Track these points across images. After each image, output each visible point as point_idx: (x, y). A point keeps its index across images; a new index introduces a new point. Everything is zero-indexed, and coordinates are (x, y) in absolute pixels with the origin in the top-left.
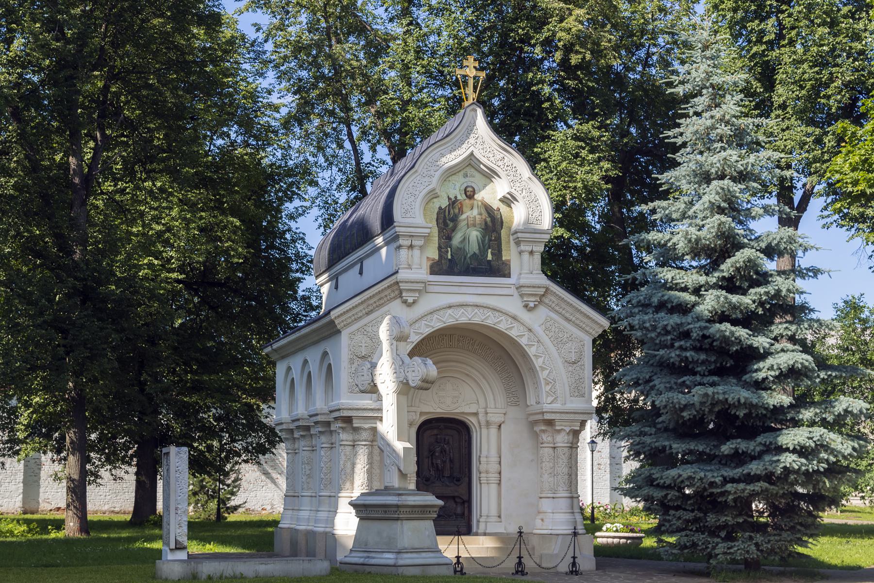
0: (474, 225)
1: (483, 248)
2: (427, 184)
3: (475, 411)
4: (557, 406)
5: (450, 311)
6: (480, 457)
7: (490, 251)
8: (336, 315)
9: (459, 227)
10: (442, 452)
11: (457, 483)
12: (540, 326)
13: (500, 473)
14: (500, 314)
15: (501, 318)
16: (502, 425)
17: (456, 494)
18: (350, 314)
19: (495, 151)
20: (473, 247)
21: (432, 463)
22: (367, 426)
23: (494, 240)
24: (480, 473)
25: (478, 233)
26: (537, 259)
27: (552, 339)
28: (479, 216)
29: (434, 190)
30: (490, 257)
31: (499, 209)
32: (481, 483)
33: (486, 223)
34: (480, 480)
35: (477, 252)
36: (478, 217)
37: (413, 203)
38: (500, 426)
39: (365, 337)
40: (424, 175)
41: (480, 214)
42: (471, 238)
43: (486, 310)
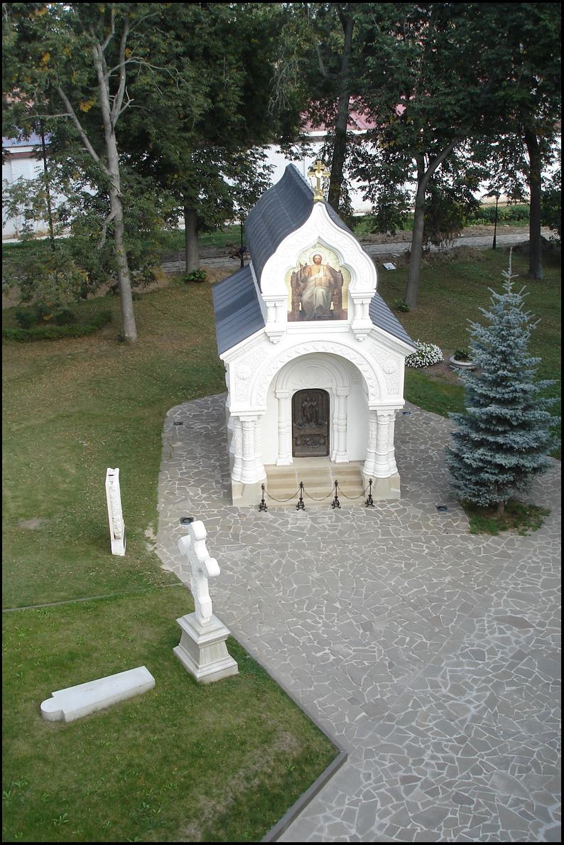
1: (327, 300)
4: (377, 402)
5: (303, 345)
7: (332, 303)
9: (309, 285)
20: (320, 301)
22: (248, 420)
25: (323, 290)
26: (367, 308)
30: (332, 308)
31: (340, 271)
33: (330, 283)
35: (322, 304)
36: (324, 278)
41: (326, 276)
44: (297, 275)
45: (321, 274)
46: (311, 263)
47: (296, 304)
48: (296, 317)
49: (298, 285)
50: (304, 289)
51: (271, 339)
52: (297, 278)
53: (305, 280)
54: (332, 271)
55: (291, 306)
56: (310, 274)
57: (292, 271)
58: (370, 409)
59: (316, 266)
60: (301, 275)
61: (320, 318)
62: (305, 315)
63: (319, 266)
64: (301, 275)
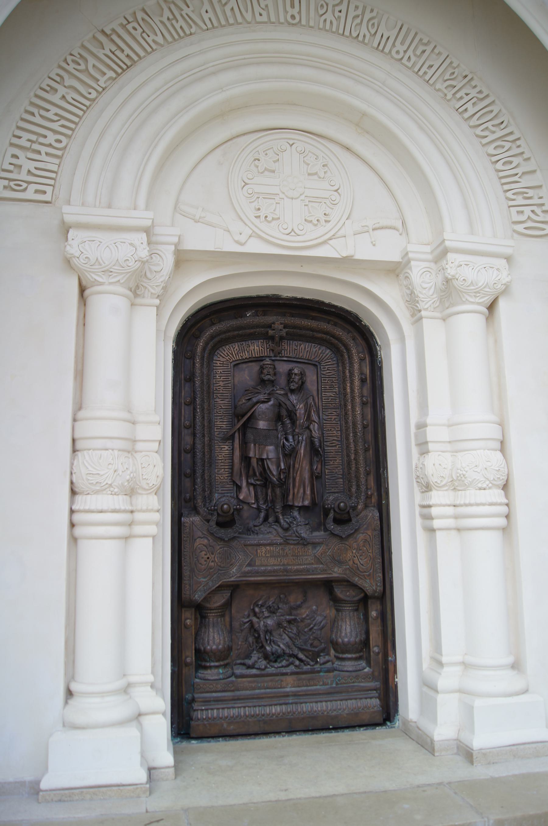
3: (396, 257)
6: (421, 426)
10: (279, 418)
11: (337, 530)
16: (502, 304)
17: (337, 572)
21: (246, 459)
24: (427, 488)
32: (431, 531)
34: (428, 517)
38: (492, 307)
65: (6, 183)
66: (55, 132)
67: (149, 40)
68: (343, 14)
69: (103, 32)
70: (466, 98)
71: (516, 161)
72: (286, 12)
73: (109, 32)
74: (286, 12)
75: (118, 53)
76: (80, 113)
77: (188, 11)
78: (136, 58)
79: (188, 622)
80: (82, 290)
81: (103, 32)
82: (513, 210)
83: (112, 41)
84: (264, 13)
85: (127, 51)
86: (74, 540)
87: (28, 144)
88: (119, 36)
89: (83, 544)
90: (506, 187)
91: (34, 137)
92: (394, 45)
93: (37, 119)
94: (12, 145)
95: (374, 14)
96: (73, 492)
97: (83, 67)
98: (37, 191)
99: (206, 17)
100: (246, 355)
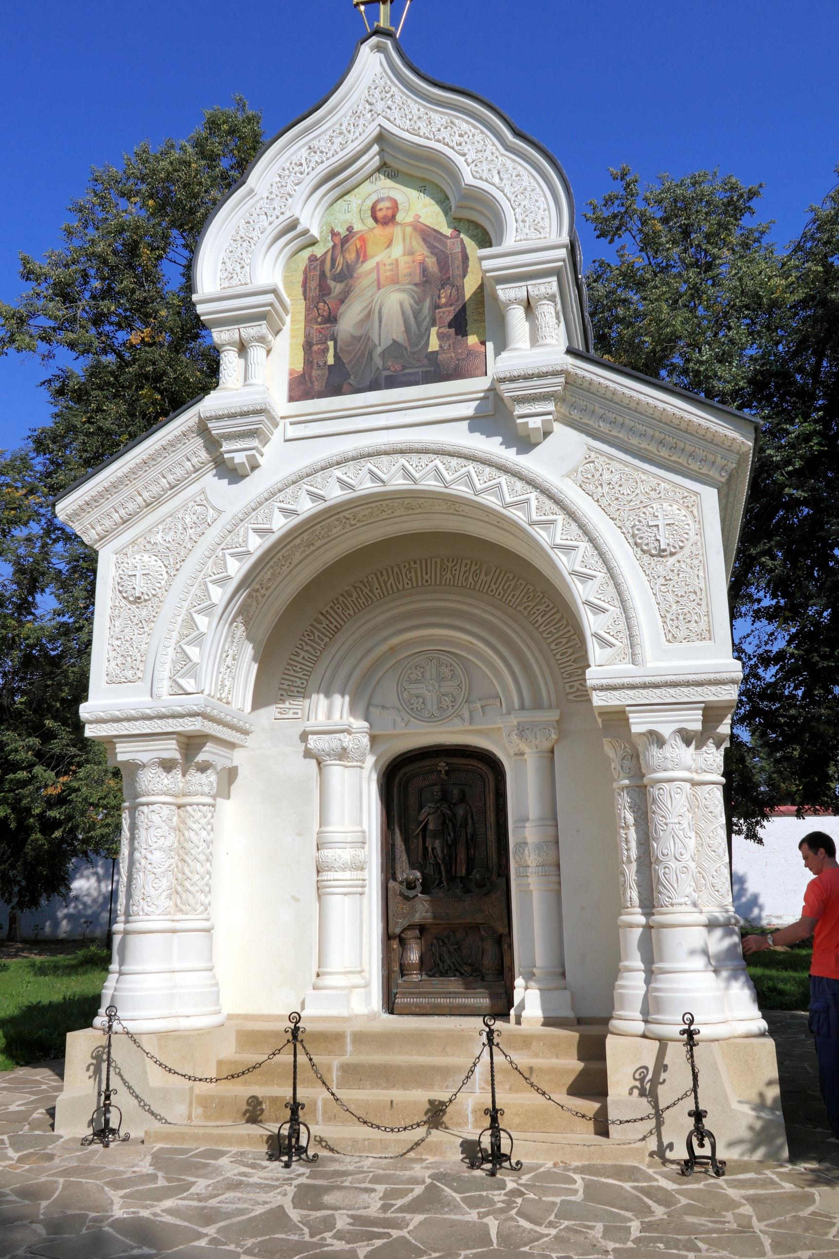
0: (395, 281)
2: (277, 212)
4: (623, 671)
5: (338, 473)
7: (434, 330)
8: (69, 511)
12: (568, 476)
13: (558, 866)
14: (460, 460)
15: (464, 470)
18: (107, 506)
19: (431, 114)
23: (445, 305)
25: (405, 297)
27: (604, 502)
28: (408, 259)
29: (293, 225)
30: (434, 344)
33: (424, 270)
36: (404, 262)
37: (244, 256)
38: (552, 751)
39: (146, 556)
40: (273, 196)
41: (410, 252)
42: (385, 312)
43: (425, 458)
44: (323, 262)
45: (397, 251)
46: (363, 225)
47: (315, 348)
48: (318, 386)
49: (324, 290)
50: (342, 301)
51: (226, 446)
52: (323, 275)
53: (346, 275)
54: (429, 236)
55: (301, 354)
56: (362, 255)
57: (306, 254)
58: (598, 700)
59: (379, 230)
60: (333, 261)
61: (392, 383)
62: (347, 375)
63: (388, 230)
64: (333, 261)
65: (279, 710)
66: (301, 679)
67: (346, 614)
68: (457, 572)
69: (321, 613)
70: (538, 613)
71: (570, 651)
72: (422, 578)
73: (325, 613)
74: (422, 578)
75: (330, 625)
76: (312, 665)
77: (366, 590)
78: (339, 627)
79: (395, 946)
80: (319, 763)
81: (321, 613)
82: (567, 686)
83: (327, 618)
84: (410, 582)
85: (335, 623)
86: (319, 896)
87: (288, 687)
88: (330, 615)
89: (324, 898)
90: (562, 670)
91: (290, 683)
92: (489, 586)
93: (292, 673)
94: (280, 689)
95: (477, 567)
96: (318, 872)
97: (312, 638)
98: (294, 713)
99: (376, 592)
100: (427, 783)
